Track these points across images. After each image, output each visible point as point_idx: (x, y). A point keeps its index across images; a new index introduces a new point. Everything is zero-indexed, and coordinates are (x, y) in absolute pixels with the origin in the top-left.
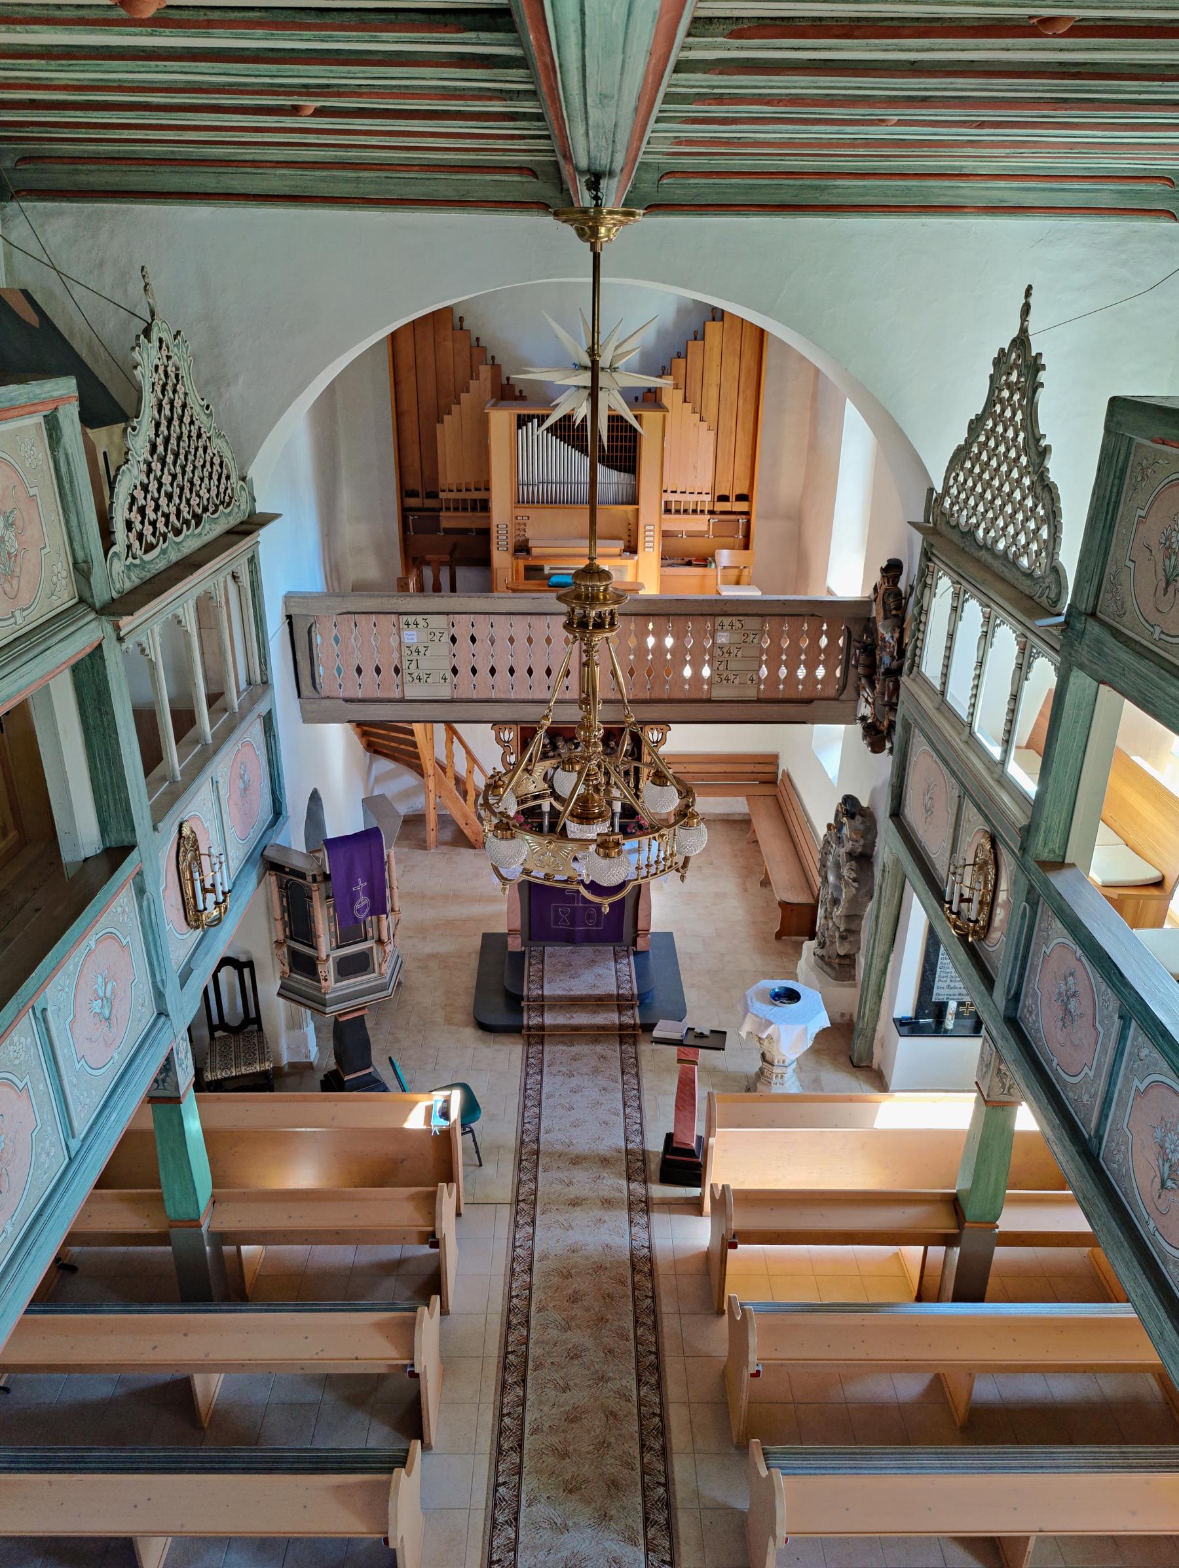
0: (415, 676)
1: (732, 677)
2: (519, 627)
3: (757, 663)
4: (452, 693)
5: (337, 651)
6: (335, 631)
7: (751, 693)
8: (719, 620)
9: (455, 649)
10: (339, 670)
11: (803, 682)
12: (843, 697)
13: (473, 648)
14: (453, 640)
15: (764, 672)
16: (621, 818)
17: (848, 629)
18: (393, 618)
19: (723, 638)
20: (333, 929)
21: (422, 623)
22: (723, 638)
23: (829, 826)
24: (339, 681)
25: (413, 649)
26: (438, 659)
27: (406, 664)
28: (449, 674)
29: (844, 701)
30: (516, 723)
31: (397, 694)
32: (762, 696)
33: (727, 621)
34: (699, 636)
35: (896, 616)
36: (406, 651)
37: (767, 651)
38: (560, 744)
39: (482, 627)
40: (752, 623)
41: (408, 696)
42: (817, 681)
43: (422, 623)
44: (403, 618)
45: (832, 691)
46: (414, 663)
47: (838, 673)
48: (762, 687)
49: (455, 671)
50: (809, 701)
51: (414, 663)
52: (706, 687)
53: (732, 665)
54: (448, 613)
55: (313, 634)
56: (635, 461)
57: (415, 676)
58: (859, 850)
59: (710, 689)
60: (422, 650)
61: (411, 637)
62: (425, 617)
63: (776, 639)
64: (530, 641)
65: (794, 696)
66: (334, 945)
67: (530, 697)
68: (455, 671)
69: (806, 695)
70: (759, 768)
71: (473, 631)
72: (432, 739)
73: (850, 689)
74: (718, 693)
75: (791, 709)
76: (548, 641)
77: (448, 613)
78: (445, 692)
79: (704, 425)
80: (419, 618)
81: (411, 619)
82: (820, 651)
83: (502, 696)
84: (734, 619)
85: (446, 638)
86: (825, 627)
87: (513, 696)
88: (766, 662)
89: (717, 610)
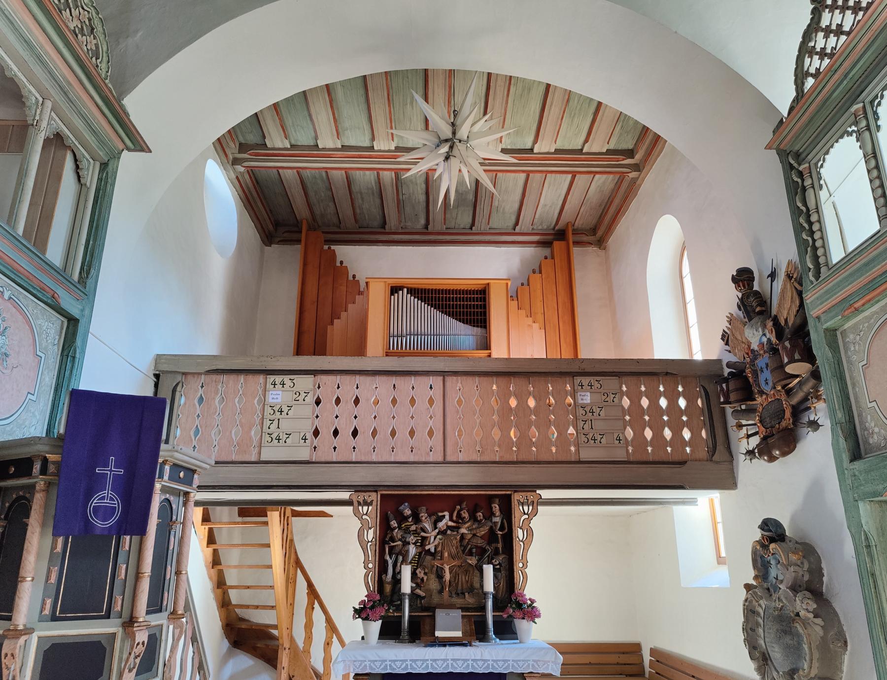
0: (274, 436)
1: (598, 437)
2: (383, 385)
3: (621, 423)
4: (311, 456)
5: (198, 412)
6: (201, 392)
7: (620, 455)
8: (578, 380)
9: (318, 410)
10: (197, 432)
11: (671, 443)
12: (716, 457)
13: (337, 410)
14: (318, 402)
15: (629, 433)
16: (494, 610)
17: (704, 387)
18: (261, 378)
19: (586, 398)
20: (53, 579)
21: (288, 383)
22: (586, 398)
23: (748, 587)
24: (194, 443)
25: (276, 409)
26: (300, 420)
27: (267, 423)
28: (309, 436)
29: (717, 463)
30: (374, 488)
31: (253, 458)
32: (632, 459)
33: (585, 381)
34: (560, 395)
35: (761, 313)
36: (268, 410)
37: (629, 412)
38: (423, 515)
39: (348, 387)
40: (610, 383)
41: (264, 458)
42: (684, 443)
43: (288, 383)
44: (271, 378)
45: (703, 453)
46: (276, 422)
47: (704, 434)
48: (630, 449)
49: (316, 433)
50: (682, 463)
51: (276, 422)
52: (573, 449)
53: (599, 425)
54: (314, 373)
55: (178, 394)
56: (485, 315)
57: (274, 436)
58: (806, 577)
59: (578, 451)
60: (285, 409)
61: (276, 396)
62: (292, 377)
63: (635, 400)
64: (394, 401)
65: (665, 459)
66: (47, 612)
67: (392, 460)
68: (316, 433)
69: (677, 458)
70: (624, 659)
71: (338, 393)
72: (292, 605)
73: (720, 447)
74: (585, 455)
75: (665, 472)
76: (413, 401)
77: (314, 373)
78: (304, 454)
79: (536, 326)
80: (287, 379)
81: (278, 379)
82: (682, 412)
83: (364, 459)
84: (592, 379)
85: (311, 399)
86: (680, 389)
87: (374, 459)
88: (630, 423)
89: (575, 368)
